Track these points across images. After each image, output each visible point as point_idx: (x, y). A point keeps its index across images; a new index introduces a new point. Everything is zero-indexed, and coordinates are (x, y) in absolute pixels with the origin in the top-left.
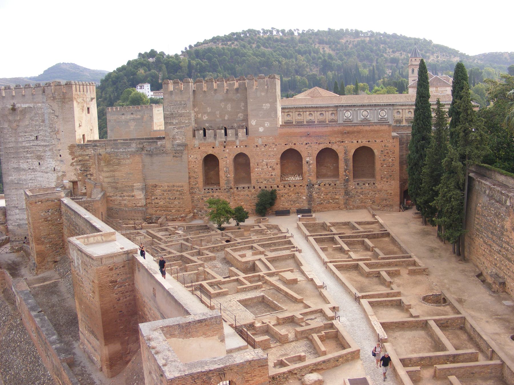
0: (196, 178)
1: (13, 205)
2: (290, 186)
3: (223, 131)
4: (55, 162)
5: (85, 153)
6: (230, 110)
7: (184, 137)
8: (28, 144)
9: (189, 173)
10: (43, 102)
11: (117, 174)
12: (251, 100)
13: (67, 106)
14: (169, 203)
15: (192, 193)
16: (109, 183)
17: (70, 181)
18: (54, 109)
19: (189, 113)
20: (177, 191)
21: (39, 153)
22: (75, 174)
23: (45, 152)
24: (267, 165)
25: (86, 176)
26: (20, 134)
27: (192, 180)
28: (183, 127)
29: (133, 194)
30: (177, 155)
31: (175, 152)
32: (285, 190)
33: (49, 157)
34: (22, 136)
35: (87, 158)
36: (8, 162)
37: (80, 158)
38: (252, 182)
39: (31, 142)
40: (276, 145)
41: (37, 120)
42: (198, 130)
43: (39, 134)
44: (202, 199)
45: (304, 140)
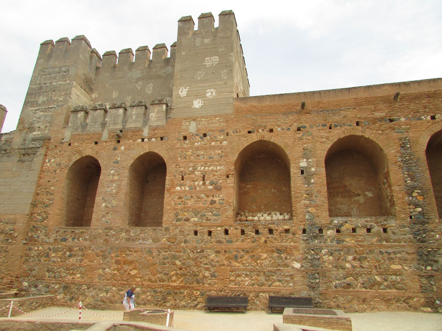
2: (257, 232)
6: (150, 92)
7: (48, 125)
12: (183, 54)
24: (204, 177)
28: (51, 108)
30: (26, 158)
31: (23, 152)
32: (243, 241)
38: (164, 219)
40: (227, 134)
44: (48, 256)
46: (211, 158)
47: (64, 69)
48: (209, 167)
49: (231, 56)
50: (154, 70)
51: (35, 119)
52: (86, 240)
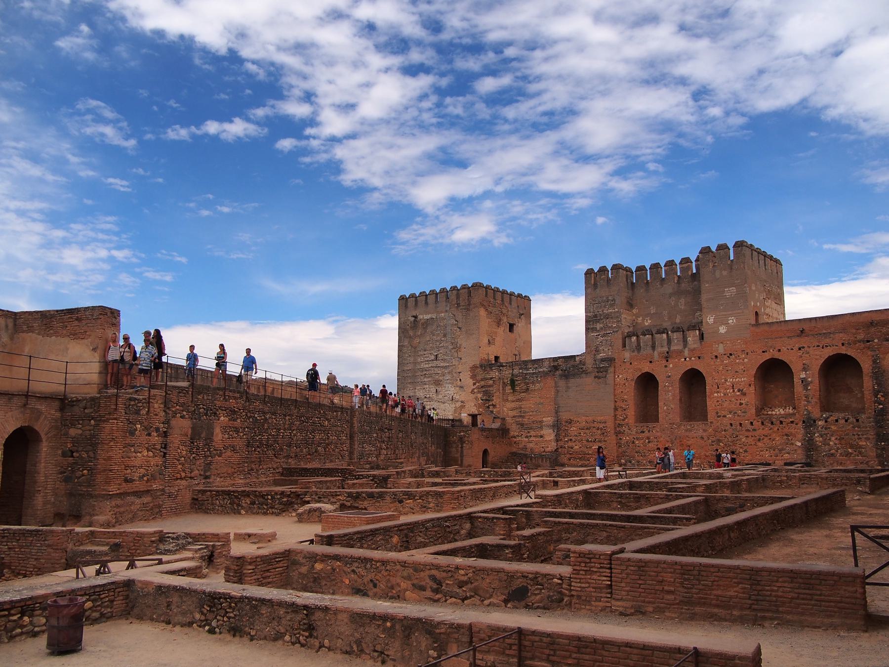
0: (625, 410)
2: (772, 423)
3: (665, 336)
9: (616, 401)
10: (446, 311)
11: (525, 405)
14: (587, 448)
15: (619, 433)
16: (514, 417)
17: (469, 415)
19: (617, 312)
20: (598, 429)
22: (475, 405)
23: (444, 375)
25: (488, 407)
27: (619, 412)
28: (609, 333)
29: (542, 432)
32: (763, 429)
34: (421, 355)
37: (482, 383)
40: (747, 354)
42: (629, 336)
44: (633, 442)
45: (796, 343)
46: (737, 372)
48: (736, 379)
49: (745, 287)
50: (683, 285)
52: (657, 431)
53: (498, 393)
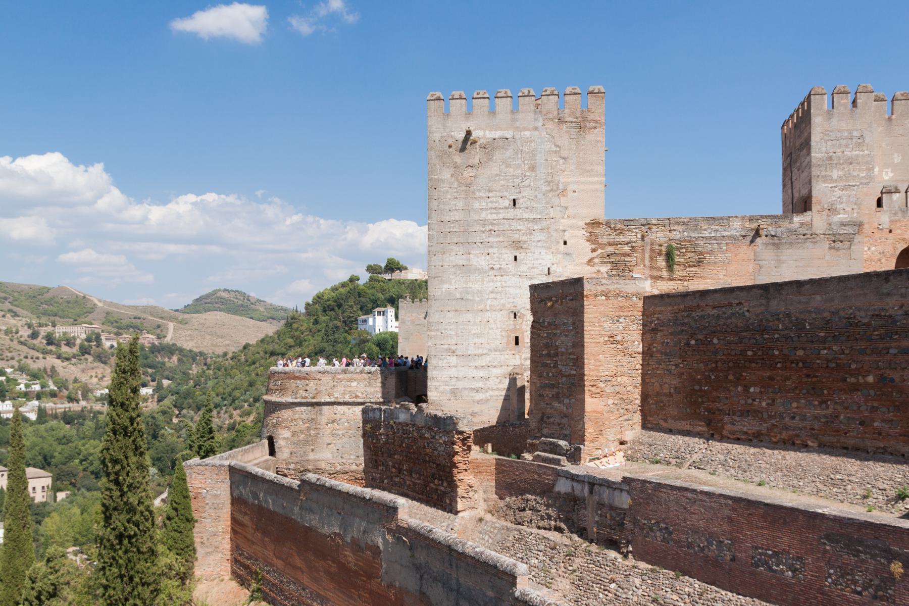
1: (446, 346)
4: (551, 256)
5: (621, 238)
7: (855, 207)
8: (494, 216)
10: (536, 129)
13: (588, 137)
18: (559, 143)
21: (517, 236)
23: (531, 234)
26: (478, 194)
28: (853, 186)
33: (539, 244)
34: (481, 198)
35: (627, 249)
36: (444, 253)
37: (610, 249)
39: (501, 211)
41: (518, 166)
43: (520, 196)
47: (855, 134)
51: (834, 199)
53: (641, 267)
